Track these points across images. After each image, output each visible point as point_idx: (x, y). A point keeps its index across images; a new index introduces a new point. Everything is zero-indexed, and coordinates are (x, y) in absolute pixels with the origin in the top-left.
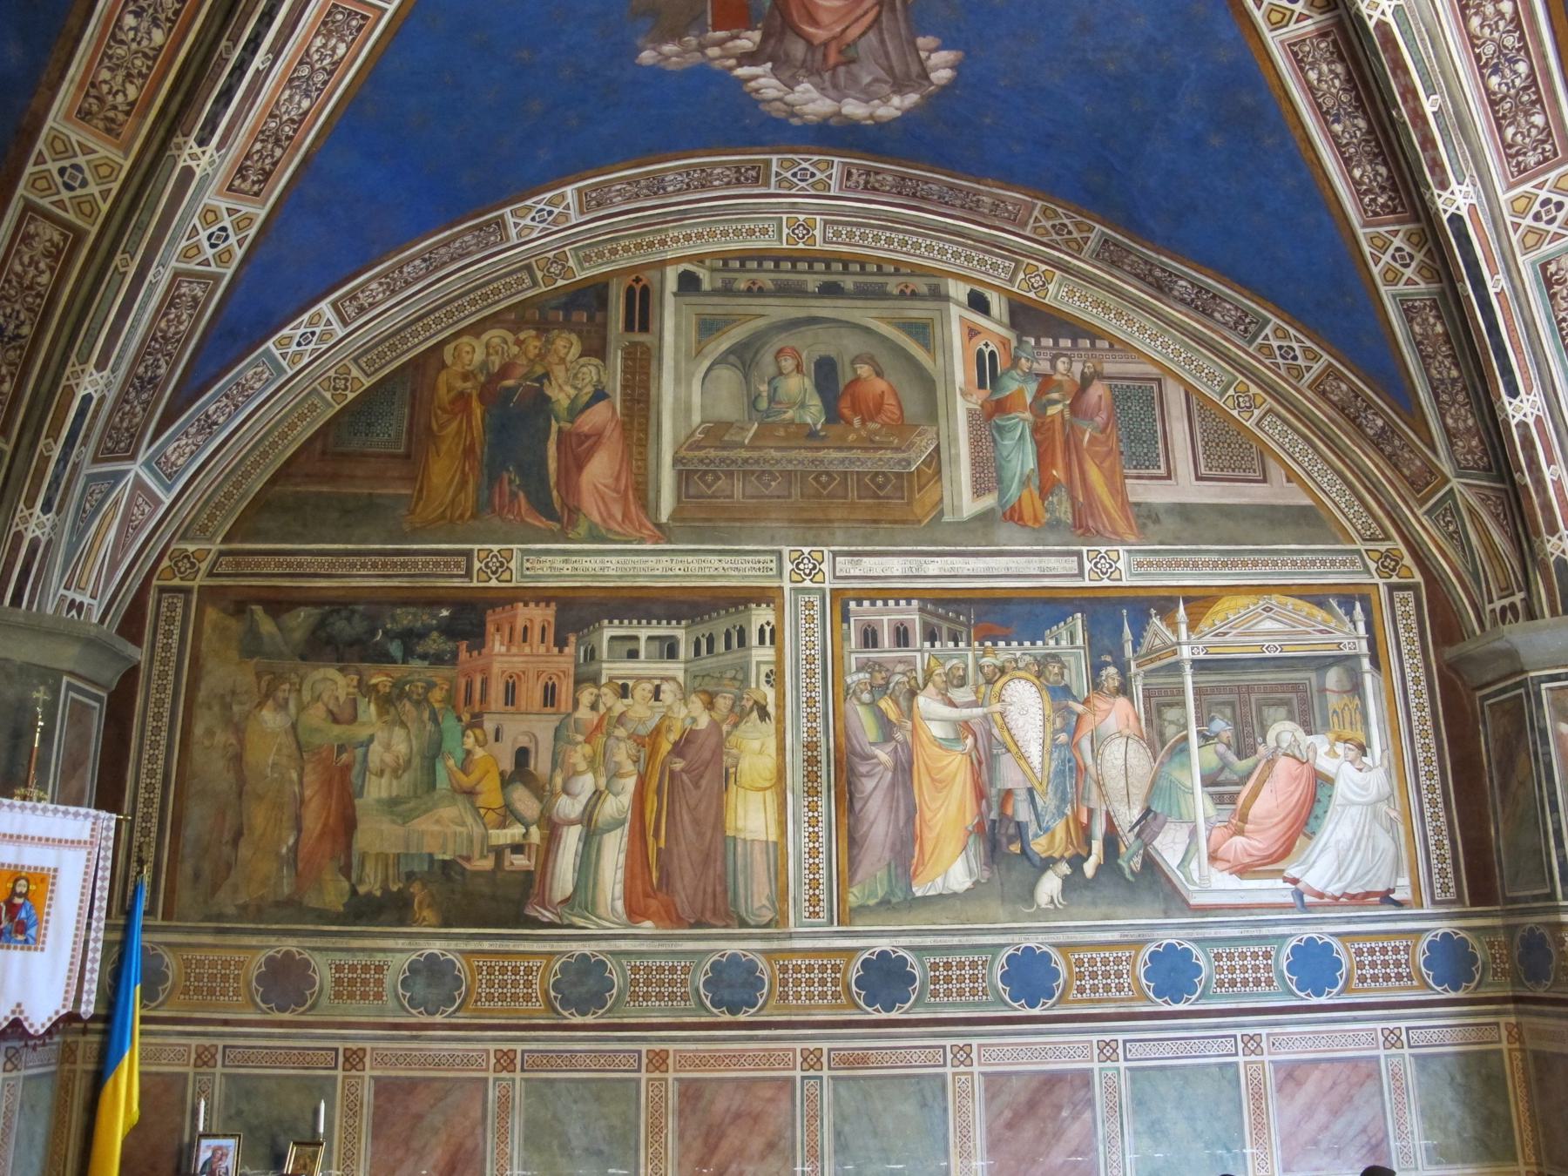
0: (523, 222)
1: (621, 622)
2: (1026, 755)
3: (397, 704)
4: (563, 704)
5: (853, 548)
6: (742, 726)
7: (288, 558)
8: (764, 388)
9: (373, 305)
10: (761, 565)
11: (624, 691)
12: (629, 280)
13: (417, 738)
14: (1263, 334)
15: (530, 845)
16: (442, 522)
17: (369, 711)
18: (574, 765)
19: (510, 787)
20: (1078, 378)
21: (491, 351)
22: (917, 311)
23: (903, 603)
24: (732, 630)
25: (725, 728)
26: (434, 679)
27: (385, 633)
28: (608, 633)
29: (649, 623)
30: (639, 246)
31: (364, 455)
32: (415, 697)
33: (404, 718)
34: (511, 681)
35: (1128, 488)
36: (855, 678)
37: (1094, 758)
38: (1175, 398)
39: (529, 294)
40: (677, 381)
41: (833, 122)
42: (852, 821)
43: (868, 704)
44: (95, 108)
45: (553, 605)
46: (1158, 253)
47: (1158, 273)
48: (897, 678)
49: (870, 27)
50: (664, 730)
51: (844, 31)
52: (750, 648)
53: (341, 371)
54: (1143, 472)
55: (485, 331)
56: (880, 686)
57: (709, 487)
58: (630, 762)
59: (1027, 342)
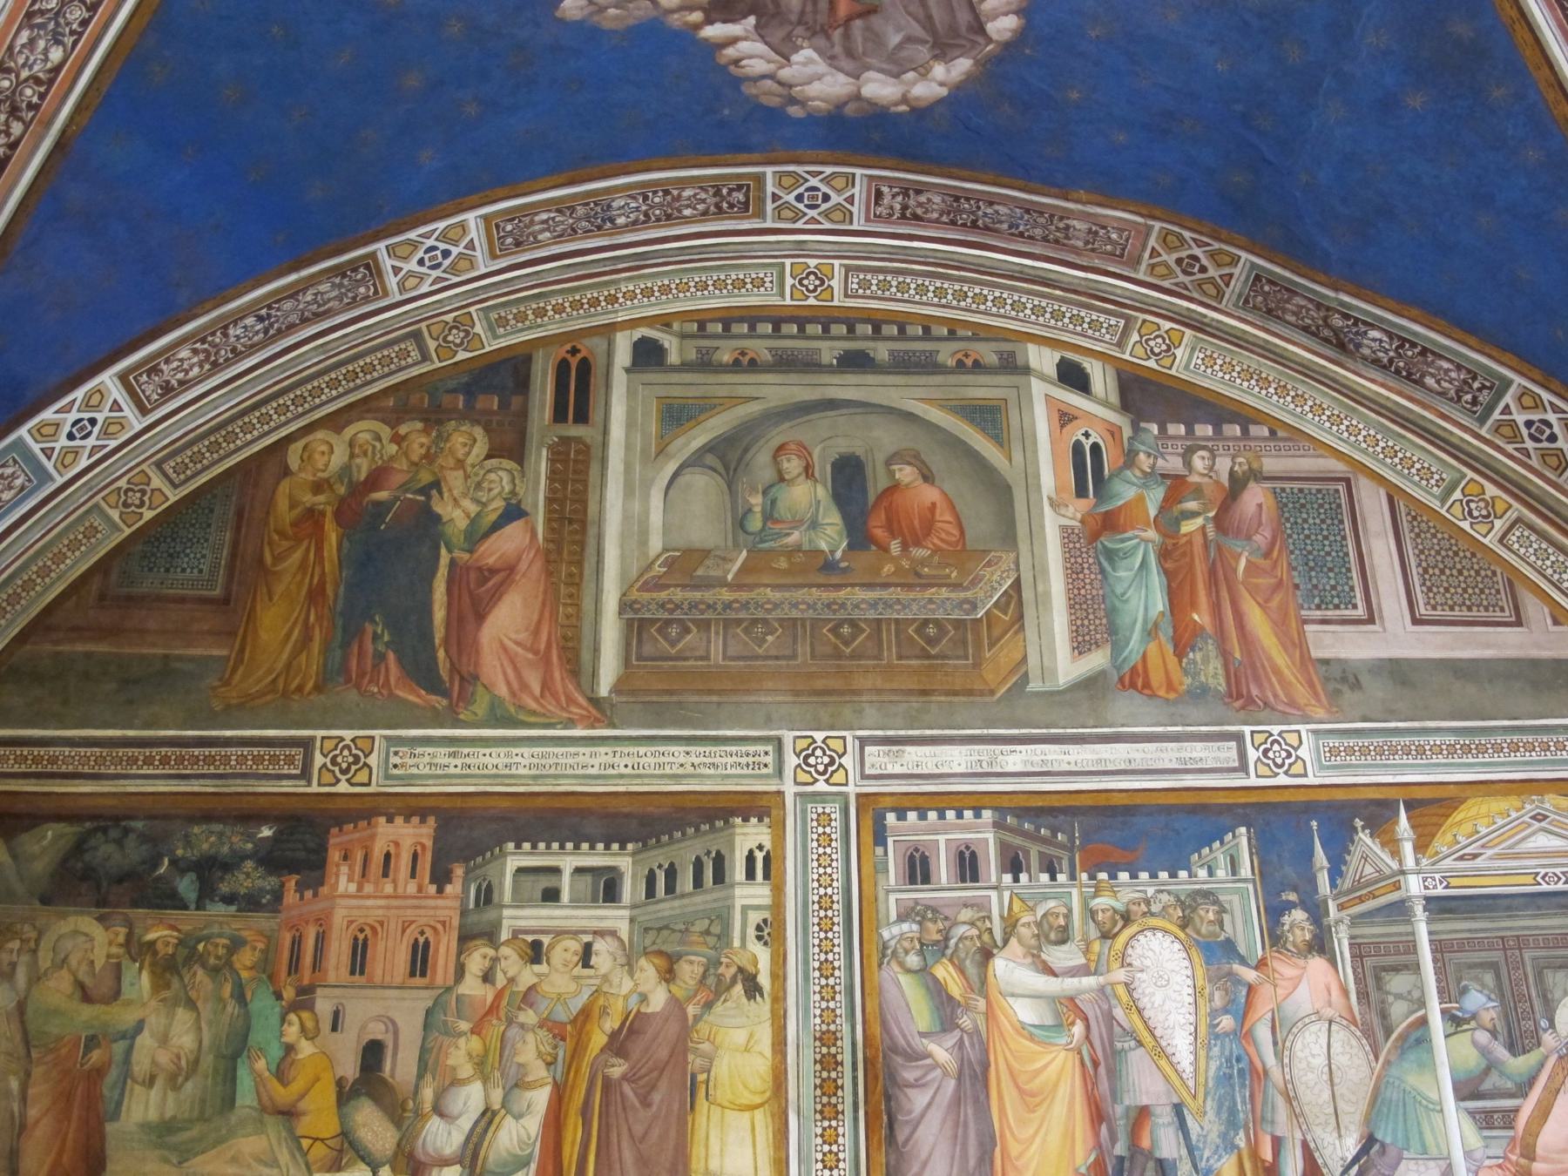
0: (406, 267)
1: (534, 847)
2: (1169, 1050)
3: (184, 971)
4: (440, 971)
5: (891, 733)
6: (719, 1008)
7: (36, 751)
8: (756, 501)
9: (185, 384)
10: (751, 760)
11: (536, 953)
12: (561, 352)
13: (210, 1023)
14: (1501, 406)
16: (269, 697)
17: (139, 982)
18: (454, 1069)
20: (1225, 479)
21: (357, 451)
22: (982, 389)
23: (968, 814)
24: (705, 859)
25: (691, 1010)
26: (245, 934)
27: (173, 862)
28: (513, 863)
29: (577, 847)
31: (159, 598)
32: (212, 961)
33: (193, 994)
34: (361, 937)
35: (1310, 637)
36: (896, 930)
37: (1279, 1055)
38: (1372, 503)
39: (415, 371)
40: (629, 491)
41: (850, 110)
42: (893, 1158)
43: (916, 972)
45: (431, 821)
46: (1336, 290)
47: (1337, 321)
48: (961, 930)
50: (596, 1011)
52: (732, 886)
53: (135, 480)
54: (1331, 614)
55: (349, 423)
56: (937, 943)
57: (673, 644)
58: (540, 1063)
59: (1146, 430)
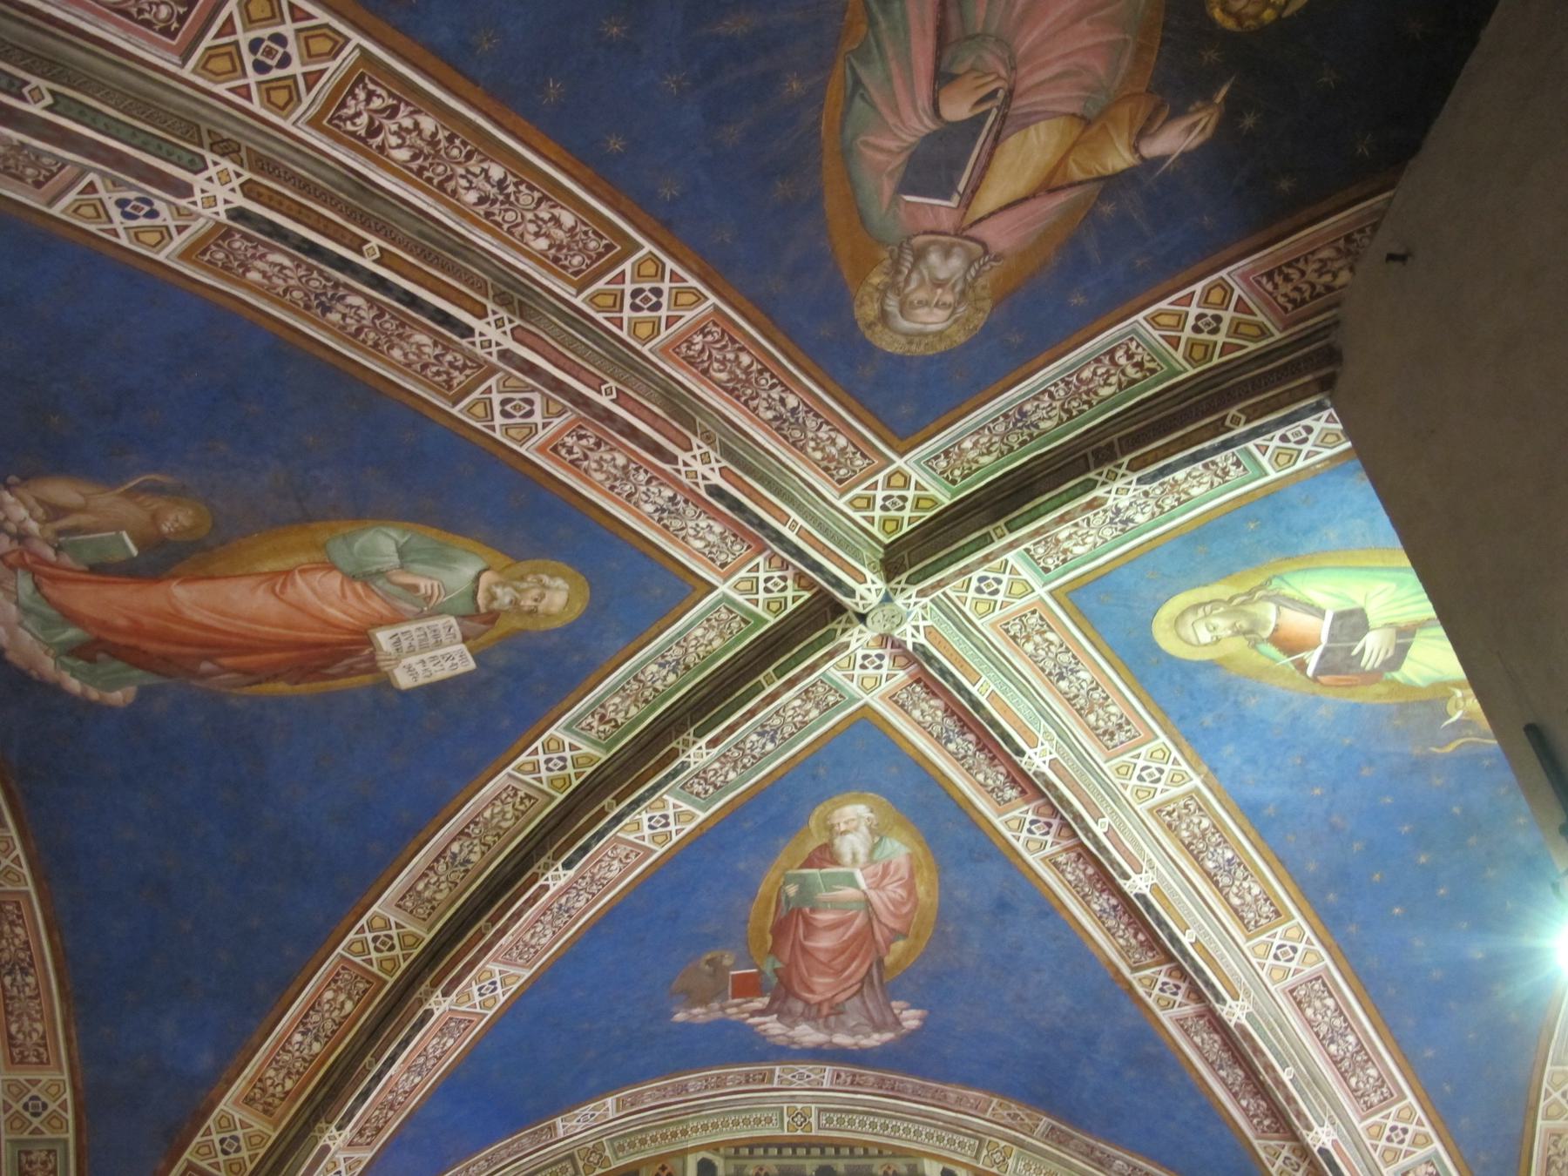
30: (664, 1137)
41: (825, 1047)
44: (258, 1096)
49: (854, 995)
51: (833, 997)
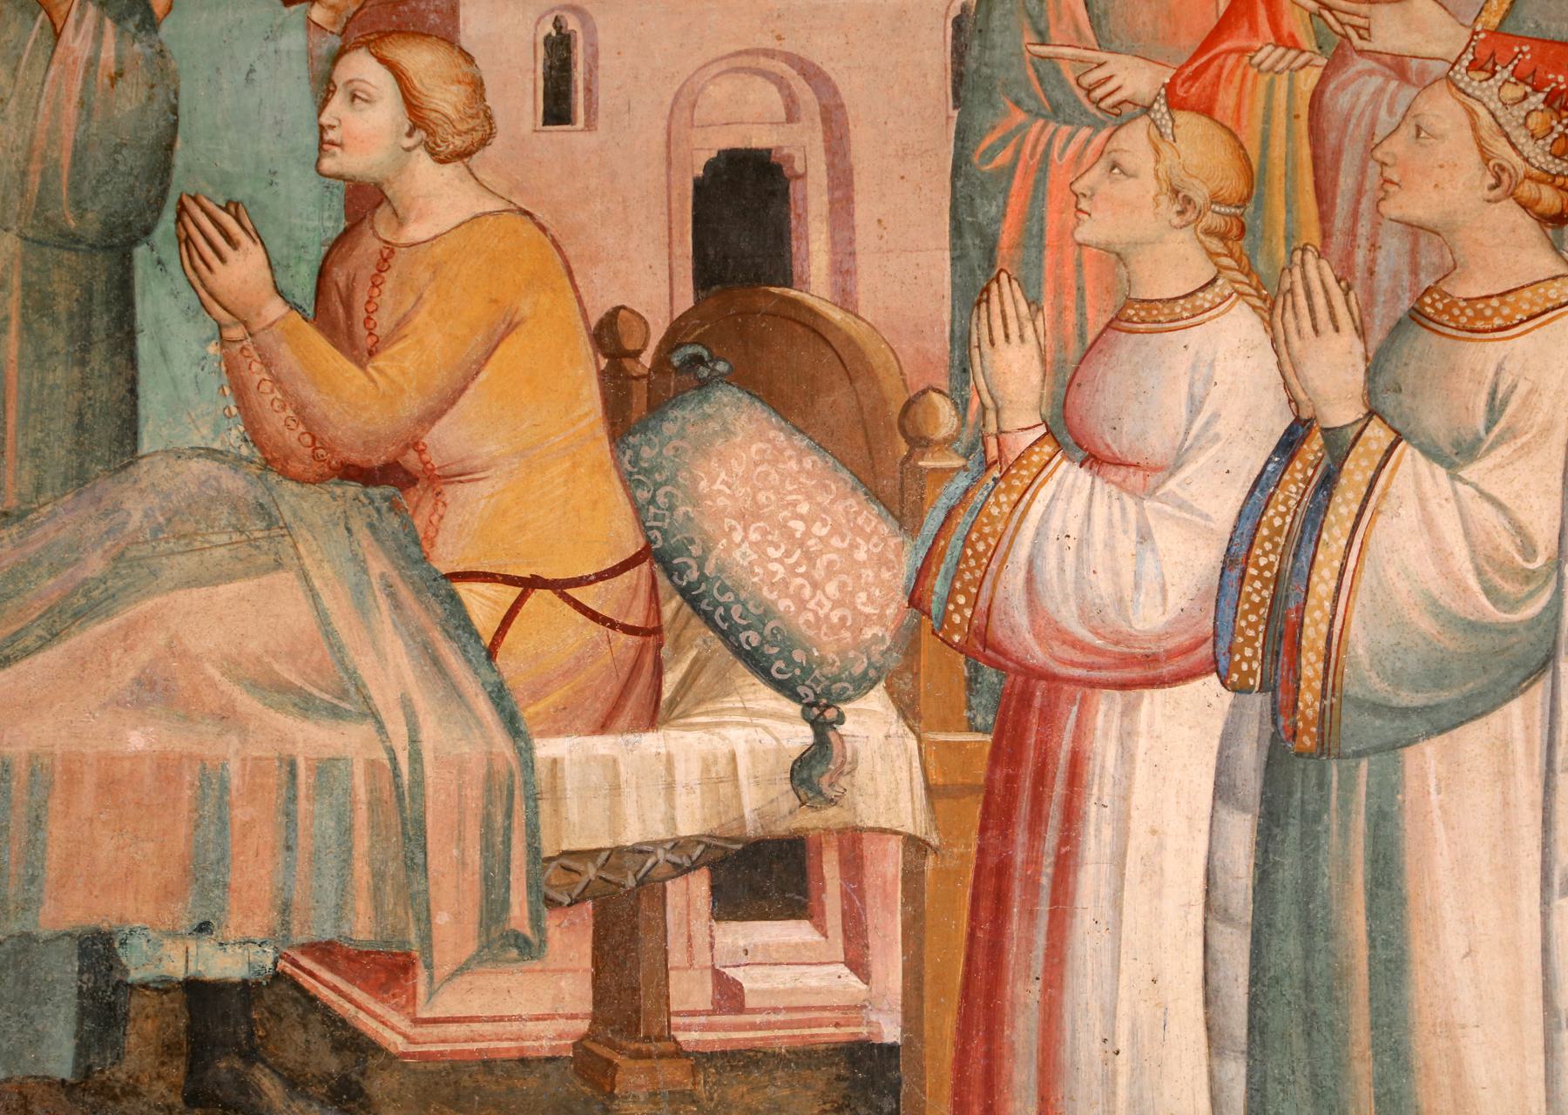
15: (852, 841)
19: (680, 420)
